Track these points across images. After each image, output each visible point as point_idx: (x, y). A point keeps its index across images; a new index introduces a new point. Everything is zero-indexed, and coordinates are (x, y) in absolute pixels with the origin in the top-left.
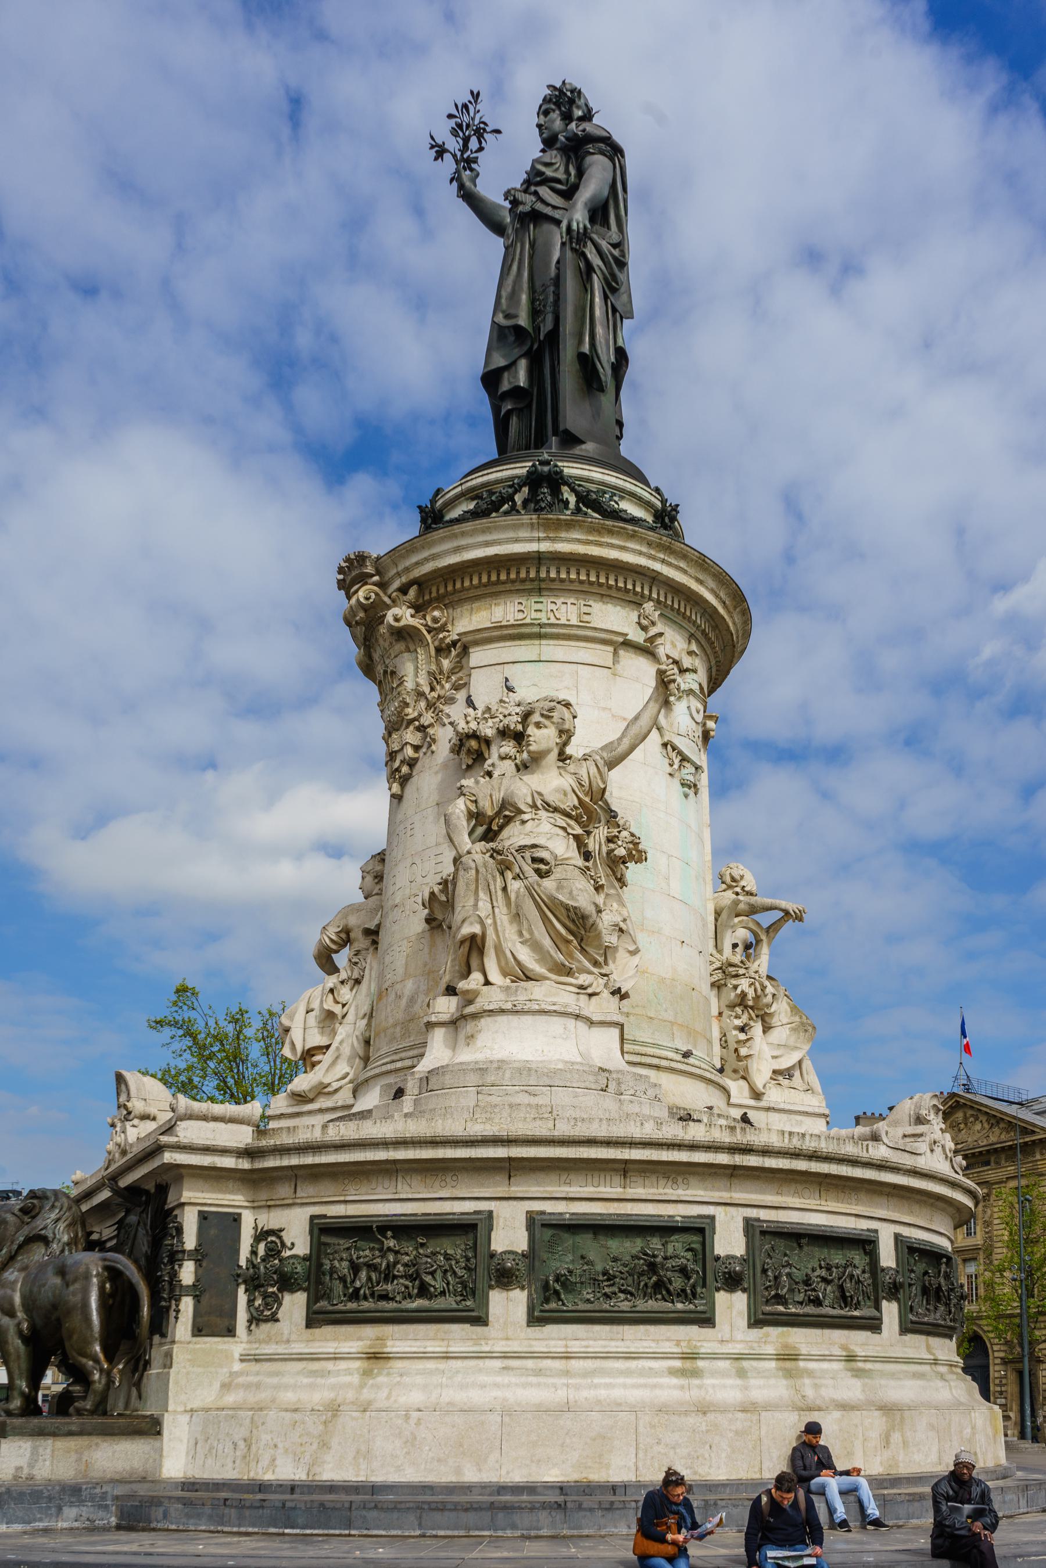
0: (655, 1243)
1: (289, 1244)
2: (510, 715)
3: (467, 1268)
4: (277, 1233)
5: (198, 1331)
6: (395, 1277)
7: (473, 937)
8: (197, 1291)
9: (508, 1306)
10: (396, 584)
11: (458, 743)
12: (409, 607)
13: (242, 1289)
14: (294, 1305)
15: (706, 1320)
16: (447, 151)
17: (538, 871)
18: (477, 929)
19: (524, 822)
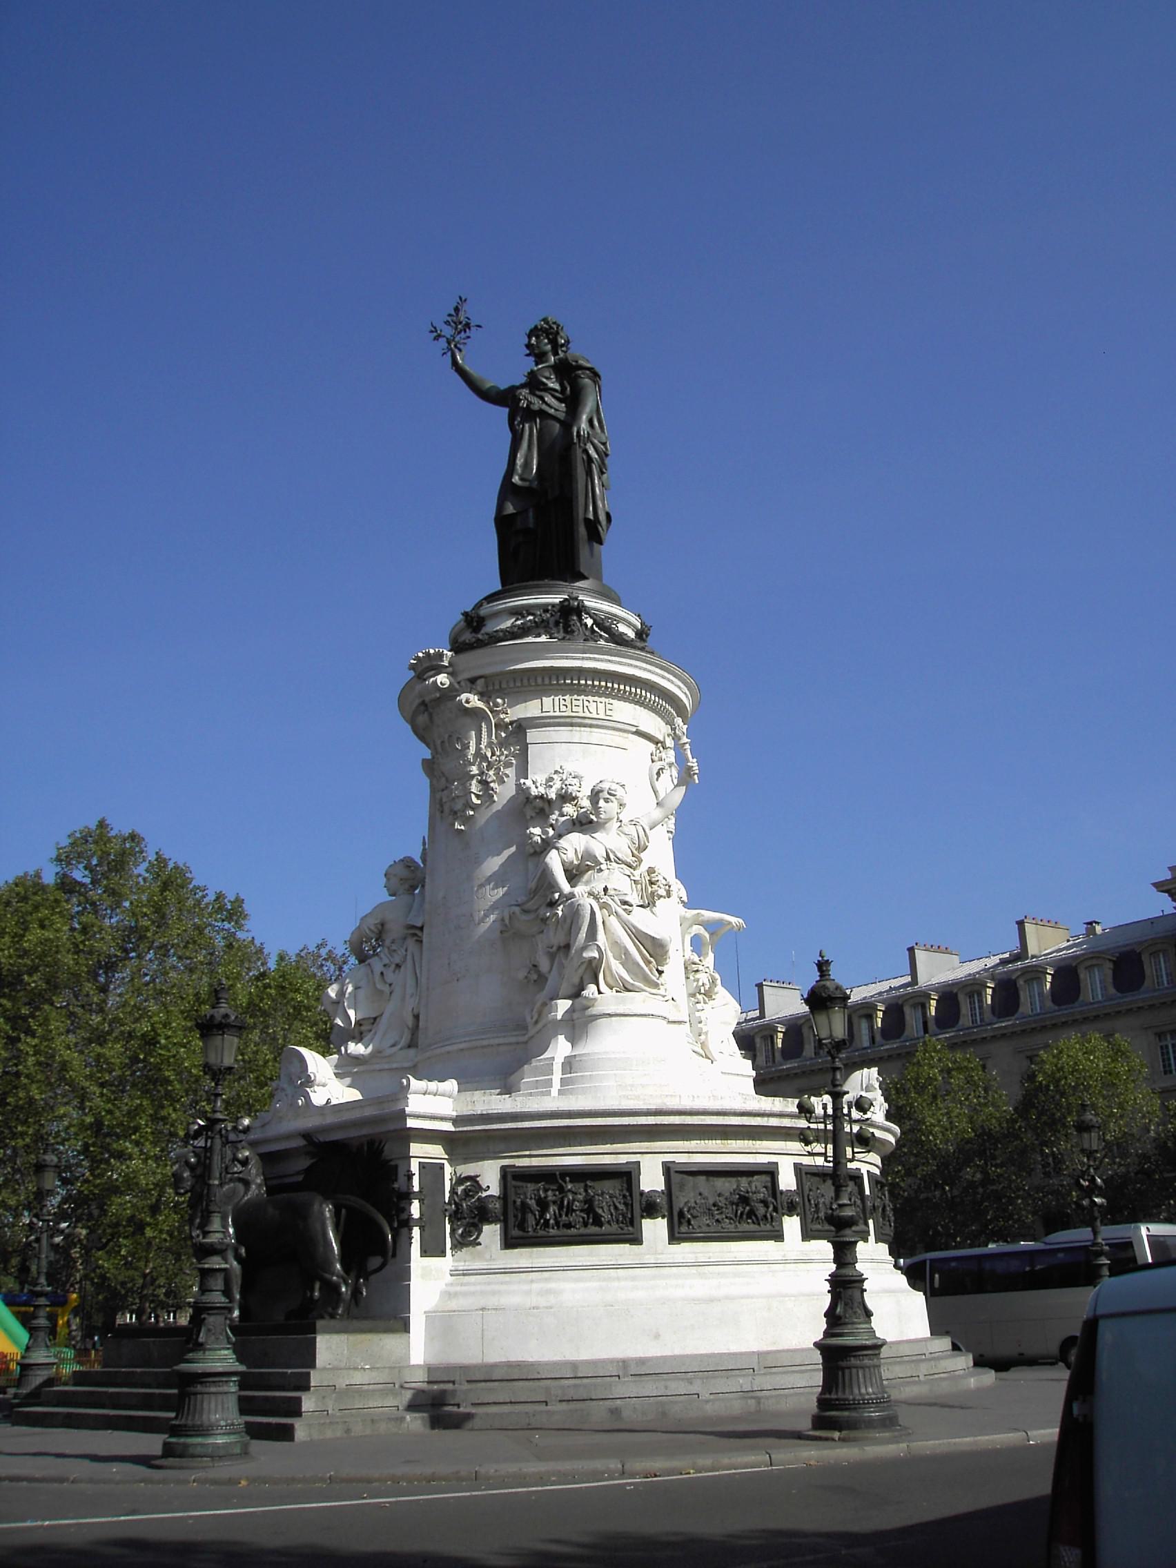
0: (744, 1181)
3: (626, 1204)
4: (473, 1179)
5: (425, 1253)
6: (574, 1211)
7: (591, 960)
8: (421, 1223)
9: (655, 1229)
10: (467, 675)
14: (491, 1233)
15: (778, 1236)
18: (596, 955)
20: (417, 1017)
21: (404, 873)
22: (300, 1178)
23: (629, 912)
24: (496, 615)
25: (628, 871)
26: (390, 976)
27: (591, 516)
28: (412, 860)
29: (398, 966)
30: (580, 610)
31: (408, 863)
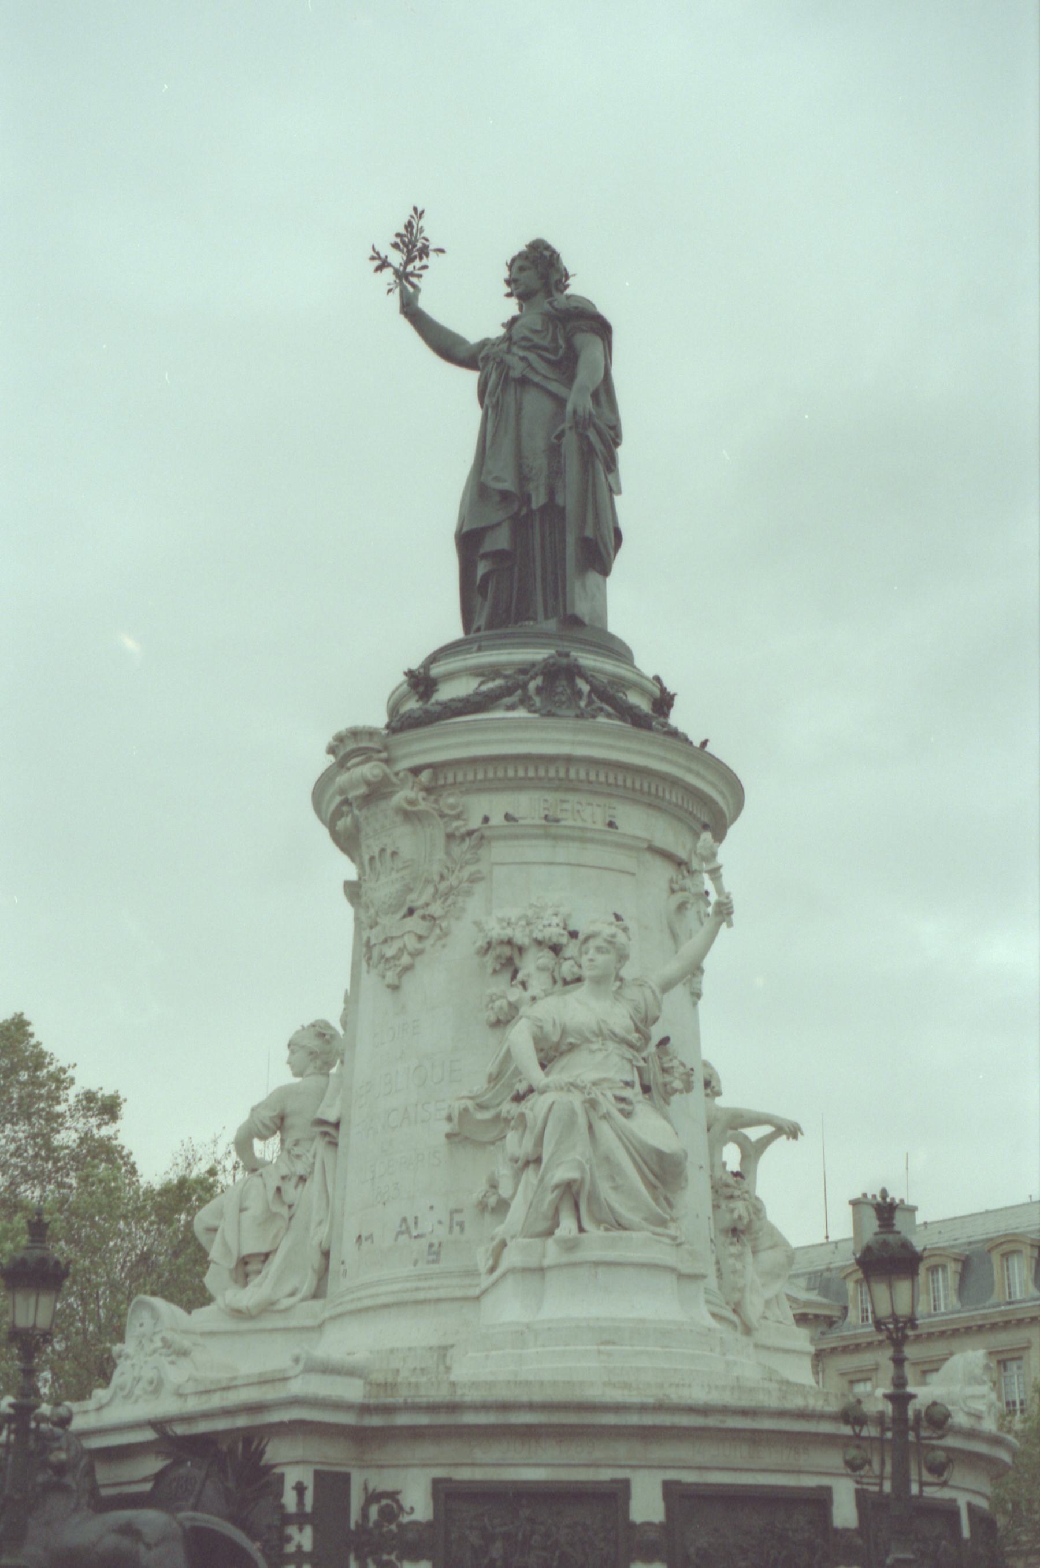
1: (408, 1509)
2: (550, 925)
4: (393, 1495)
11: (485, 945)
12: (421, 790)
13: (352, 1557)
16: (389, 265)
17: (622, 1111)
19: (592, 1052)
20: (326, 1255)
21: (315, 1044)
22: (148, 1487)
23: (628, 1115)
24: (451, 676)
25: (629, 1053)
26: (290, 1192)
27: (589, 533)
28: (327, 1025)
29: (302, 1179)
30: (574, 671)
31: (321, 1031)
